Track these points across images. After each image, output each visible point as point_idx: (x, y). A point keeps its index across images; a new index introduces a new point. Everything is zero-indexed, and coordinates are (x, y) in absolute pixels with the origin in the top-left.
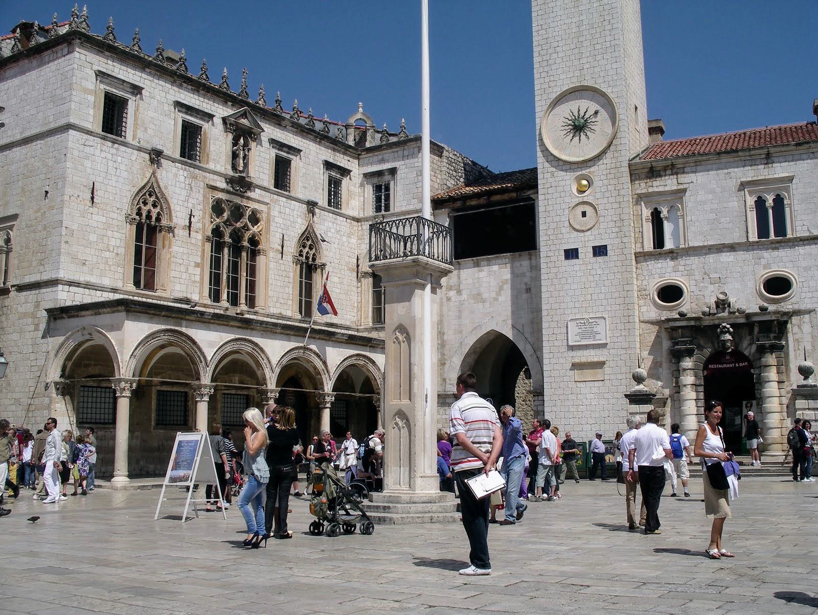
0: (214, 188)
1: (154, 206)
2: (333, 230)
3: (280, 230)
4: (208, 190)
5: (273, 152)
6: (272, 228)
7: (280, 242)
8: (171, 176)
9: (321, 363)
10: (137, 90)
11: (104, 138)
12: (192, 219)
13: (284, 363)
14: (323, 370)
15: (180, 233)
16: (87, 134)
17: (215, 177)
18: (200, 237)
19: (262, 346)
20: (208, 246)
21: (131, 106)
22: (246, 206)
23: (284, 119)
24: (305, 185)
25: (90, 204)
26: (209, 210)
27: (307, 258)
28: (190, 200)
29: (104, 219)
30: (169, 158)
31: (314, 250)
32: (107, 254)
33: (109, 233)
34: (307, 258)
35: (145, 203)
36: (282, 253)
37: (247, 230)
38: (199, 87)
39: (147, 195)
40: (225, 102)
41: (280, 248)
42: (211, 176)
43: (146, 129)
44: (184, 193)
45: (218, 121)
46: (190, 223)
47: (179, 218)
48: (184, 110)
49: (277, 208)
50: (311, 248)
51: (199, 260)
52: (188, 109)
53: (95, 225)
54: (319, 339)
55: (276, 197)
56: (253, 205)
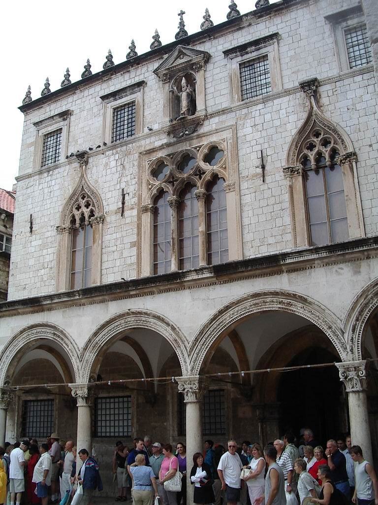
1: (87, 206)
3: (259, 148)
4: (144, 157)
5: (234, 64)
7: (259, 162)
8: (101, 168)
9: (169, 329)
10: (65, 115)
12: (127, 197)
14: (176, 340)
16: (29, 178)
20: (147, 218)
22: (196, 148)
24: (293, 70)
25: (29, 234)
29: (40, 242)
31: (332, 145)
33: (45, 251)
35: (78, 208)
36: (264, 176)
39: (80, 199)
41: (260, 170)
42: (148, 141)
45: (152, 81)
46: (123, 203)
47: (110, 202)
48: (112, 99)
49: (249, 123)
50: (325, 143)
51: (134, 238)
53: (33, 249)
54: (160, 292)
55: (244, 111)
56: (205, 142)
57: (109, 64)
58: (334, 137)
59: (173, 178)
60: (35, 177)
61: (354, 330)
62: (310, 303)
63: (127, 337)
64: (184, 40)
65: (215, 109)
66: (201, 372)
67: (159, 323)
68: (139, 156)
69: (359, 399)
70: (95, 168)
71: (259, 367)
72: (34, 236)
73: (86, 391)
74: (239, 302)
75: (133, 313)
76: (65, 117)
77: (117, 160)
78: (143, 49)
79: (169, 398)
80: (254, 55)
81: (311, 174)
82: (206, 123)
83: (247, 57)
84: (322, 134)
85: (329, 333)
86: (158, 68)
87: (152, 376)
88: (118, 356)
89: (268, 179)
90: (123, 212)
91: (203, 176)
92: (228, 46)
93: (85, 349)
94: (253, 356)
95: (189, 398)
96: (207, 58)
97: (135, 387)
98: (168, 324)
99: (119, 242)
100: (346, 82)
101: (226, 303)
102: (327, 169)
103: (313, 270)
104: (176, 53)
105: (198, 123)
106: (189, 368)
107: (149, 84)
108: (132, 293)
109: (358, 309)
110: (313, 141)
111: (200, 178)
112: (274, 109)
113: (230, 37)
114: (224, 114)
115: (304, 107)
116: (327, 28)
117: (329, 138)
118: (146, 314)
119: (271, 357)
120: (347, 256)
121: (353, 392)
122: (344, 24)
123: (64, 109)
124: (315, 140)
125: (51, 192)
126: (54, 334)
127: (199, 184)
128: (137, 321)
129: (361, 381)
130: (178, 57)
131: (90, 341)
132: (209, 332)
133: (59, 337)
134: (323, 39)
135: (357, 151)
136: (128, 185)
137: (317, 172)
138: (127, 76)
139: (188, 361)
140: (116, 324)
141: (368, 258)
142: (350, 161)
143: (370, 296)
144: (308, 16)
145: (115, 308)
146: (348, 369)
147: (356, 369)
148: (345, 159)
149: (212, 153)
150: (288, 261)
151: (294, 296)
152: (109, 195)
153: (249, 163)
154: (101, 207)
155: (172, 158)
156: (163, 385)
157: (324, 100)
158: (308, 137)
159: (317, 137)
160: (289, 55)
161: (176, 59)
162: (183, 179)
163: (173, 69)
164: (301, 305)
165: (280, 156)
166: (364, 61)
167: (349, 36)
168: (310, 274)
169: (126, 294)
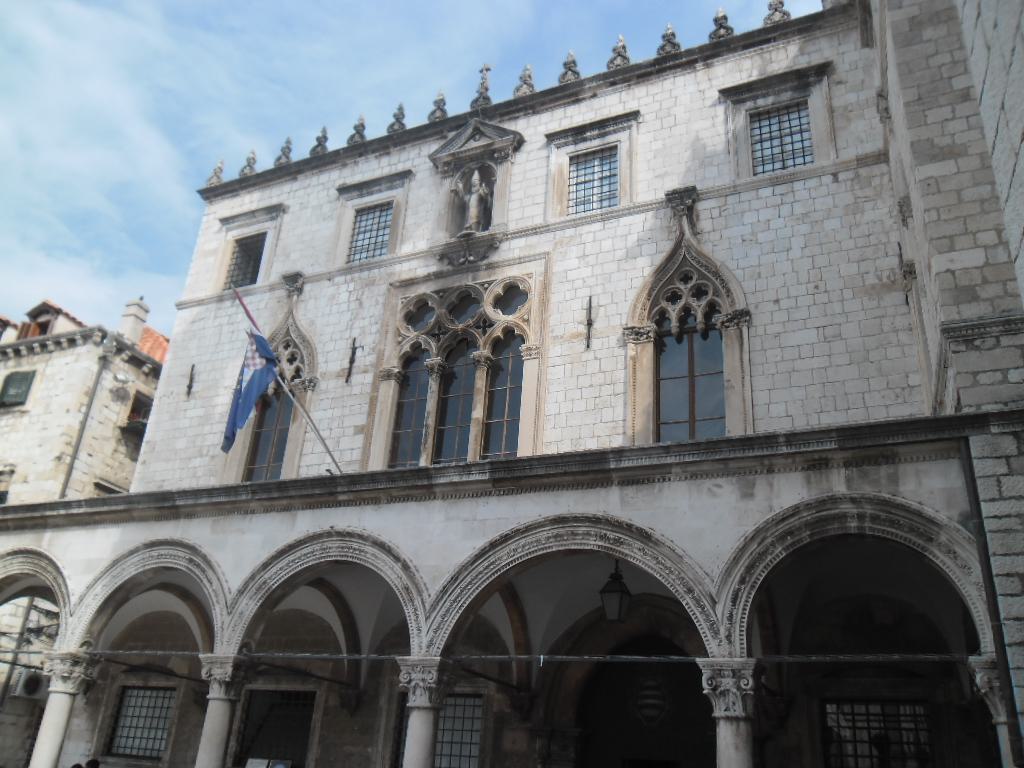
1: (291, 360)
2: (776, 223)
5: (561, 157)
6: (554, 298)
7: (582, 316)
9: (398, 567)
10: (276, 211)
12: (359, 353)
13: (274, 584)
14: (407, 589)
15: (329, 386)
17: (414, 263)
18: (369, 378)
19: (205, 550)
20: (389, 391)
22: (482, 284)
23: (581, 83)
25: (183, 397)
28: (358, 324)
30: (317, 278)
31: (710, 296)
32: (197, 462)
33: (207, 429)
36: (588, 338)
37: (491, 325)
39: (281, 349)
41: (583, 329)
42: (406, 266)
43: (288, 256)
44: (348, 316)
46: (352, 361)
47: (329, 359)
48: (355, 194)
49: (575, 251)
50: (699, 293)
55: (569, 232)
57: (357, 138)
58: (713, 284)
59: (440, 329)
60: (210, 306)
61: (734, 600)
62: (657, 543)
63: (319, 578)
64: (485, 112)
65: (522, 225)
66: (447, 651)
67: (383, 556)
68: (389, 290)
69: (737, 734)
70: (312, 302)
71: (552, 651)
72: (192, 402)
73: (229, 670)
74: (529, 529)
75: (339, 534)
76: (274, 214)
77: (350, 292)
78: (414, 120)
79: (383, 701)
81: (669, 341)
82: (504, 246)
83: (583, 147)
84: (695, 277)
85: (687, 601)
86: (437, 152)
87: (358, 651)
88: (303, 617)
89: (595, 343)
90: (349, 375)
91: (489, 331)
92: (555, 127)
93: (241, 592)
94: (541, 630)
95: (418, 699)
96: (519, 143)
97: (327, 675)
98: (397, 559)
99: (335, 424)
100: (745, 196)
101: (505, 529)
102: (697, 337)
103: (666, 484)
104: (470, 131)
105: (492, 245)
106: (425, 641)
107: (419, 176)
108: (342, 498)
109: (744, 562)
110: (679, 289)
111: (485, 332)
112: (619, 233)
113: (559, 113)
114: (536, 233)
115: (670, 232)
117: (706, 285)
118: (360, 537)
119: (575, 639)
120: (732, 465)
121: (728, 718)
122: (749, 104)
123: (274, 201)
124: (682, 287)
125: (233, 332)
126: (191, 561)
127: (481, 342)
128: (342, 548)
129: (744, 697)
130: (472, 137)
131: (252, 577)
132: (468, 579)
133: (198, 566)
134: (714, 125)
135: (752, 309)
136: (364, 332)
137: (679, 340)
138: (385, 160)
139: (424, 629)
140: (305, 551)
141: (770, 471)
142: (737, 324)
143: (769, 540)
144: (692, 88)
145: (308, 522)
146: (718, 672)
147: (736, 674)
148: (729, 321)
149: (512, 296)
150: (625, 464)
151: (628, 528)
152: (330, 346)
154: (313, 365)
155: (441, 297)
156: (377, 668)
157: (704, 224)
158: (670, 281)
159: (686, 282)
160: (654, 148)
161: (466, 142)
162: (456, 331)
163: (461, 155)
164: (638, 544)
166: (778, 165)
167: (757, 125)
168: (660, 490)
169: (331, 498)
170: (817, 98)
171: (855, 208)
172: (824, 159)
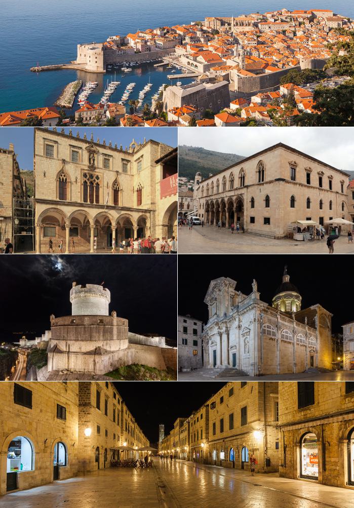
0: (84, 170)
1: (65, 176)
10: (56, 142)
11: (47, 157)
18: (80, 184)
20: (82, 187)
21: (55, 148)
26: (82, 176)
27: (116, 188)
33: (50, 185)
34: (116, 188)
35: (62, 176)
38: (77, 139)
40: (86, 143)
52: (74, 146)
56: (97, 174)
80: (107, 158)
105: (95, 168)
116: (121, 160)
153: (105, 184)
165: (111, 185)
170: (129, 164)
171: (131, 180)
172: (129, 173)
